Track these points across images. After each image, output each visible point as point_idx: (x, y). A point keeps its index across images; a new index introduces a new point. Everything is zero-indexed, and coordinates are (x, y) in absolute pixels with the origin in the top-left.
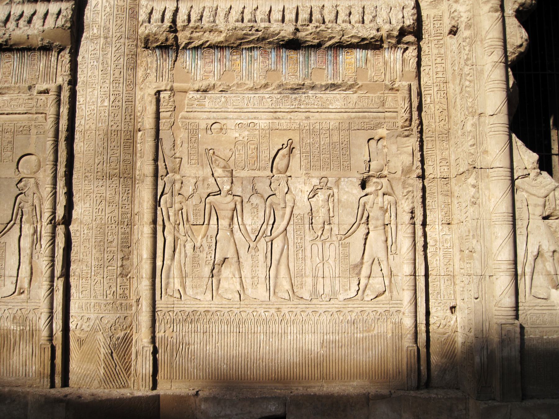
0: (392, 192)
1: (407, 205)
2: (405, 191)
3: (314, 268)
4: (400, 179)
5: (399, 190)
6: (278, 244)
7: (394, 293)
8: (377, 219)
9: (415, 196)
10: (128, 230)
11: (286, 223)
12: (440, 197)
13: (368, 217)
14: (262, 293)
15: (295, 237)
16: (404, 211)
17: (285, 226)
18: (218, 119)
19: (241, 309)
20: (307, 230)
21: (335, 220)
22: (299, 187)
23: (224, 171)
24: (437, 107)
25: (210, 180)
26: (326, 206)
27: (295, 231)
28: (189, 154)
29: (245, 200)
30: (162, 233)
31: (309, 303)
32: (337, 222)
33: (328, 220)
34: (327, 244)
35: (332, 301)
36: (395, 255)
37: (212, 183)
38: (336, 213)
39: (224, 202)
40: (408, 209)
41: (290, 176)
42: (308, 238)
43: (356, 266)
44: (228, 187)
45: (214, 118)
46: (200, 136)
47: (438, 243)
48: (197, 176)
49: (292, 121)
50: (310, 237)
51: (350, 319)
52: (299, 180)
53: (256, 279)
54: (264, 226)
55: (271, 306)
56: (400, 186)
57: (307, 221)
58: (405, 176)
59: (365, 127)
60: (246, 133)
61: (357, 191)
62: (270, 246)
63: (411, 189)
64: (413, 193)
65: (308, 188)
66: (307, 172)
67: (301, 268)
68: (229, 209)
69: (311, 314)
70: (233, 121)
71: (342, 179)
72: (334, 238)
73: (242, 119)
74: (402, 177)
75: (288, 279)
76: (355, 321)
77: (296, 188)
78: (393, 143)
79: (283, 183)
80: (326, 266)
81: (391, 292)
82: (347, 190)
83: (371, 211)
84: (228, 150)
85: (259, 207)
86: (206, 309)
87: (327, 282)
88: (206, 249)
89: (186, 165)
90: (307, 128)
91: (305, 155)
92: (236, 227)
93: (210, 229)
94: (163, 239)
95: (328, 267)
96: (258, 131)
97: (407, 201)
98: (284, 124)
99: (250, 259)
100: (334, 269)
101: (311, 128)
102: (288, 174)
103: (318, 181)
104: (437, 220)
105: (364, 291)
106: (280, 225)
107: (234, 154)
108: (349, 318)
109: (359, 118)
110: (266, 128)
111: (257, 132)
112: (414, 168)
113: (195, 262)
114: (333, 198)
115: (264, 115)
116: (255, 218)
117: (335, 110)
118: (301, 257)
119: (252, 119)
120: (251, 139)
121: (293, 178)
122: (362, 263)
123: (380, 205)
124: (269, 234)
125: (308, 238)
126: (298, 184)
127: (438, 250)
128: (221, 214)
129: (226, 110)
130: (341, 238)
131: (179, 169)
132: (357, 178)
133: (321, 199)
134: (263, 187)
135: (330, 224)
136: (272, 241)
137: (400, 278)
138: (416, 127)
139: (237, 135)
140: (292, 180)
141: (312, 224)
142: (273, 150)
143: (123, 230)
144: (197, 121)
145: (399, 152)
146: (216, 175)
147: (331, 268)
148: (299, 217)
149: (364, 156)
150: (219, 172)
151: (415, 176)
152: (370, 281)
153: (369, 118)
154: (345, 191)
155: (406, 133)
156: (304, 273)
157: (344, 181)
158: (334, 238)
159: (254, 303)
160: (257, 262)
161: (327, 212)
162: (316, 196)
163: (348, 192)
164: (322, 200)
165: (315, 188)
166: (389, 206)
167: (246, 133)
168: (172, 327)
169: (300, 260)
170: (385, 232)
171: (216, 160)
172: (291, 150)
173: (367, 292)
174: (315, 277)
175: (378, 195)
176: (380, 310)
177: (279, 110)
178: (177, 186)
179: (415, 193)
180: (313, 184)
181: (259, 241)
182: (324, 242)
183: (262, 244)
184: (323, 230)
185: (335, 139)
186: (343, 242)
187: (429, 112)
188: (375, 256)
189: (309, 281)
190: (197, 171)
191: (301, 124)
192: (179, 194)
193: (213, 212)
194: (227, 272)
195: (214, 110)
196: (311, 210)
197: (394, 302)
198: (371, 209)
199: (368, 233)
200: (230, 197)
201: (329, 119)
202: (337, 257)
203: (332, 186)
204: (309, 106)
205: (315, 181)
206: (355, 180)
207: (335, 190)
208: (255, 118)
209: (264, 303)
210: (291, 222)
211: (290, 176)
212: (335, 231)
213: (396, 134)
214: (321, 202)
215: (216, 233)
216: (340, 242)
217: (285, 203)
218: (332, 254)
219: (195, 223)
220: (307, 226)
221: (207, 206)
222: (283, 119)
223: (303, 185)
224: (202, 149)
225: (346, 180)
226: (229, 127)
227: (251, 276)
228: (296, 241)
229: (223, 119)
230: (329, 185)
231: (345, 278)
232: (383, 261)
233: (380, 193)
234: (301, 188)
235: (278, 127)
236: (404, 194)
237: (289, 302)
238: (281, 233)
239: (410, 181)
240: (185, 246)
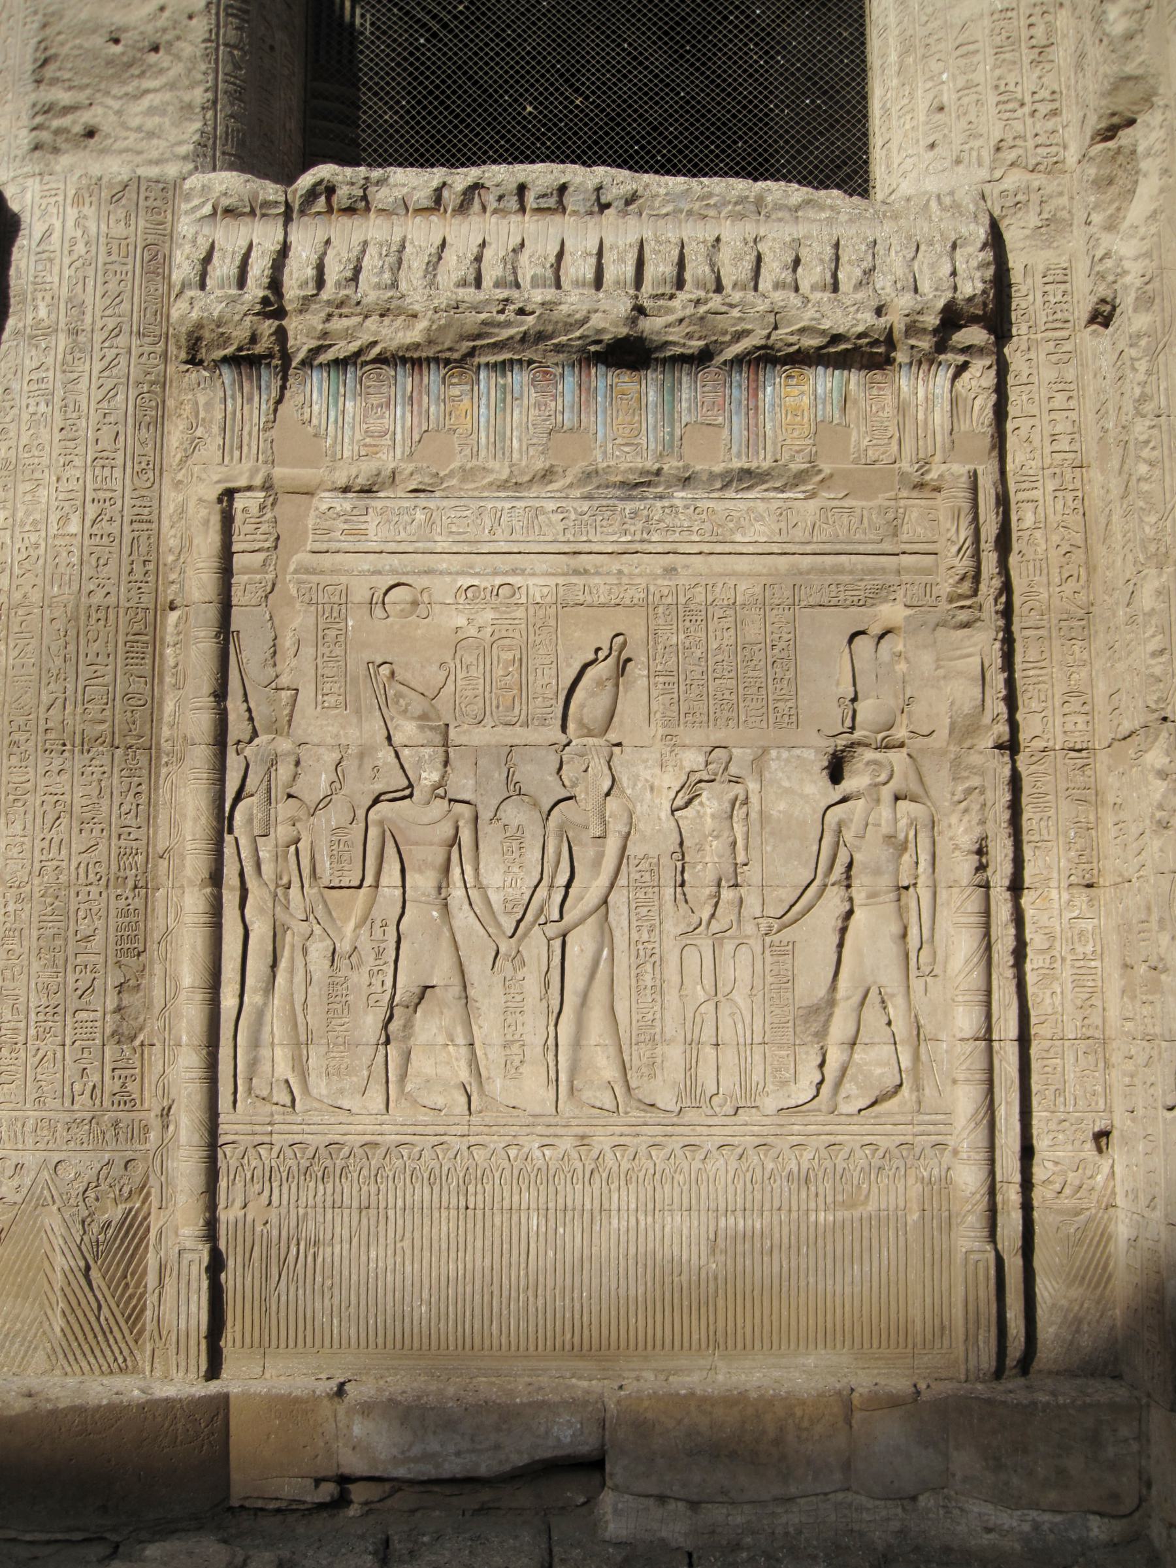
0: (921, 792)
1: (966, 831)
2: (960, 788)
3: (690, 1015)
4: (944, 752)
5: (942, 787)
6: (581, 946)
7: (927, 1091)
8: (877, 872)
9: (989, 804)
10: (138, 903)
11: (607, 884)
12: (1064, 805)
13: (850, 866)
14: (533, 1090)
15: (634, 924)
16: (957, 847)
17: (604, 891)
18: (407, 574)
19: (473, 1140)
20: (669, 905)
21: (752, 874)
22: (646, 774)
23: (421, 728)
24: (1055, 538)
25: (380, 755)
26: (726, 834)
27: (633, 905)
28: (319, 679)
29: (485, 815)
30: (237, 912)
31: (675, 1120)
32: (756, 879)
33: (732, 875)
34: (729, 947)
35: (743, 1116)
36: (929, 979)
37: (385, 764)
38: (755, 854)
39: (424, 821)
40: (967, 841)
41: (619, 744)
42: (672, 928)
43: (814, 1010)
44: (435, 777)
45: (394, 572)
46: (350, 623)
47: (1057, 944)
48: (344, 742)
49: (625, 580)
50: (676, 925)
51: (795, 1170)
53: (515, 1049)
54: (542, 893)
55: (560, 1131)
56: (945, 773)
57: (668, 877)
58: (960, 743)
59: (842, 597)
60: (489, 615)
61: (818, 789)
62: (558, 952)
63: (975, 781)
64: (982, 793)
65: (670, 780)
66: (668, 731)
67: (650, 1016)
68: (436, 840)
69: (679, 1152)
70: (448, 579)
72: (749, 928)
73: (478, 574)
74: (952, 748)
75: (612, 1050)
76: (812, 1174)
77: (636, 777)
78: (925, 647)
79: (598, 764)
80: (725, 1010)
81: (918, 1088)
82: (786, 784)
83: (859, 849)
84: (435, 668)
85: (527, 834)
86: (368, 1138)
87: (729, 1057)
88: (370, 959)
89: (310, 711)
90: (669, 600)
91: (661, 679)
92: (457, 893)
93: (380, 899)
94: (241, 931)
95: (732, 1014)
96: (522, 608)
97: (966, 818)
98: (601, 588)
99: (498, 990)
100: (748, 1020)
101: (682, 600)
102: (613, 736)
103: (701, 759)
104: (1055, 875)
105: (838, 1085)
106: (590, 889)
107: (452, 677)
108: (793, 1165)
109: (823, 571)
110: (549, 599)
111: (520, 613)
112: (987, 719)
113: (336, 995)
114: (744, 809)
115: (542, 564)
116: (516, 869)
117: (751, 549)
118: (649, 983)
119: (506, 574)
120: (504, 634)
121: (627, 750)
122: (831, 1002)
123: (886, 829)
124: (555, 916)
125: (672, 928)
126: (641, 767)
127: (1057, 965)
128: (413, 855)
129: (430, 546)
131: (290, 721)
132: (818, 750)
133: (709, 811)
134: (537, 776)
135: (736, 885)
136: (564, 936)
137: (945, 1045)
138: (991, 598)
139: (461, 621)
140: (625, 757)
141: (683, 884)
142: (569, 665)
143: (122, 903)
144: (343, 579)
145: (941, 672)
146: (397, 739)
147: (738, 1017)
148: (644, 865)
149: (838, 684)
150: (407, 730)
151: (990, 744)
152: (856, 1056)
153: (851, 572)
155: (963, 616)
156: (658, 1030)
157: (778, 758)
158: (749, 928)
159: (511, 1121)
160: (519, 998)
161: (729, 851)
162: (696, 802)
163: (788, 791)
164: (713, 816)
165: (695, 778)
166: (912, 834)
167: (489, 615)
168: (266, 1193)
169: (648, 991)
170: (901, 911)
171: (399, 695)
172: (622, 667)
173: (848, 1087)
174: (692, 1044)
175: (878, 801)
176: (884, 1143)
177: (586, 547)
178: (284, 771)
179: (989, 794)
181: (525, 935)
182: (717, 940)
183: (536, 946)
184: (717, 903)
185: (753, 632)
186: (776, 938)
187: (1030, 555)
188: (870, 980)
189: (675, 1054)
190: (343, 728)
191: (652, 589)
192: (290, 796)
193: (390, 850)
194: (430, 1027)
195: (392, 547)
196: (681, 844)
197: (927, 1118)
198: (857, 842)
199: (850, 913)
200: (440, 806)
201: (734, 574)
202: (758, 982)
203: (742, 773)
204: (676, 537)
205: (693, 759)
206: (810, 755)
207: (753, 786)
208: (514, 572)
209: (540, 1120)
210: (622, 881)
211: (619, 744)
212: (753, 905)
213: (932, 619)
214: (709, 820)
215: (399, 911)
216: (768, 939)
217: (604, 823)
218: (744, 975)
219: (335, 883)
221: (373, 832)
222: (597, 573)
223: (657, 771)
224: (356, 664)
226: (437, 597)
227: (501, 1041)
228: (635, 936)
229: (419, 573)
230: (733, 770)
231: (781, 1046)
232: (893, 996)
233: (886, 793)
234: (652, 778)
235: (581, 599)
236: (956, 798)
237: (614, 1119)
238: (591, 914)
239: (975, 759)
240: (305, 951)
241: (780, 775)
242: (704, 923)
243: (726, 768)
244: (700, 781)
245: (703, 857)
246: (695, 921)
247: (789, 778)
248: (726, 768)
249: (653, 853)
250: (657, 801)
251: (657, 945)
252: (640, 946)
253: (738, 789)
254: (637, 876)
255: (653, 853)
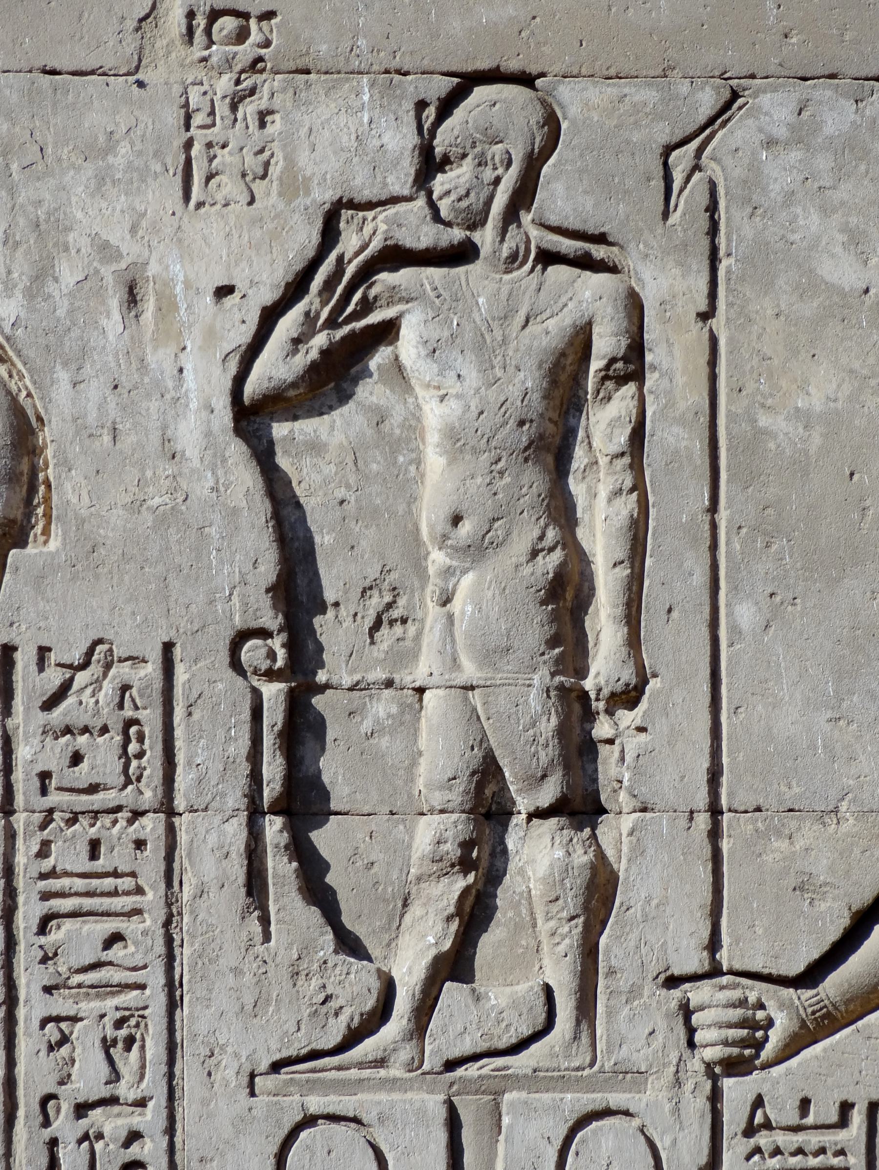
34: (529, 1126)
38: (676, 645)
52: (100, 108)
57: (214, 754)
71: (772, 108)
72: (636, 1025)
82: (841, 271)
103: (399, 140)
126: (79, 182)
130: (754, 1029)
148: (91, 700)
154: (810, 285)
157: (801, 135)
158: (636, 1025)
161: (534, 628)
165: (355, 241)
180: (326, 173)
186: (780, 1085)
207: (666, 282)
212: (658, 921)
214: (435, 461)
216: (736, 1091)
220: (213, 842)
225: (836, 114)
230: (562, 196)
241: (810, 221)
242: (403, 1004)
243: (524, 195)
244: (395, 257)
245: (406, 655)
246: (355, 987)
247: (856, 240)
248: (524, 195)
249: (136, 634)
250: (160, 359)
251: (151, 1119)
252: (64, 1125)
253: (589, 295)
254: (54, 755)
255: (136, 634)
